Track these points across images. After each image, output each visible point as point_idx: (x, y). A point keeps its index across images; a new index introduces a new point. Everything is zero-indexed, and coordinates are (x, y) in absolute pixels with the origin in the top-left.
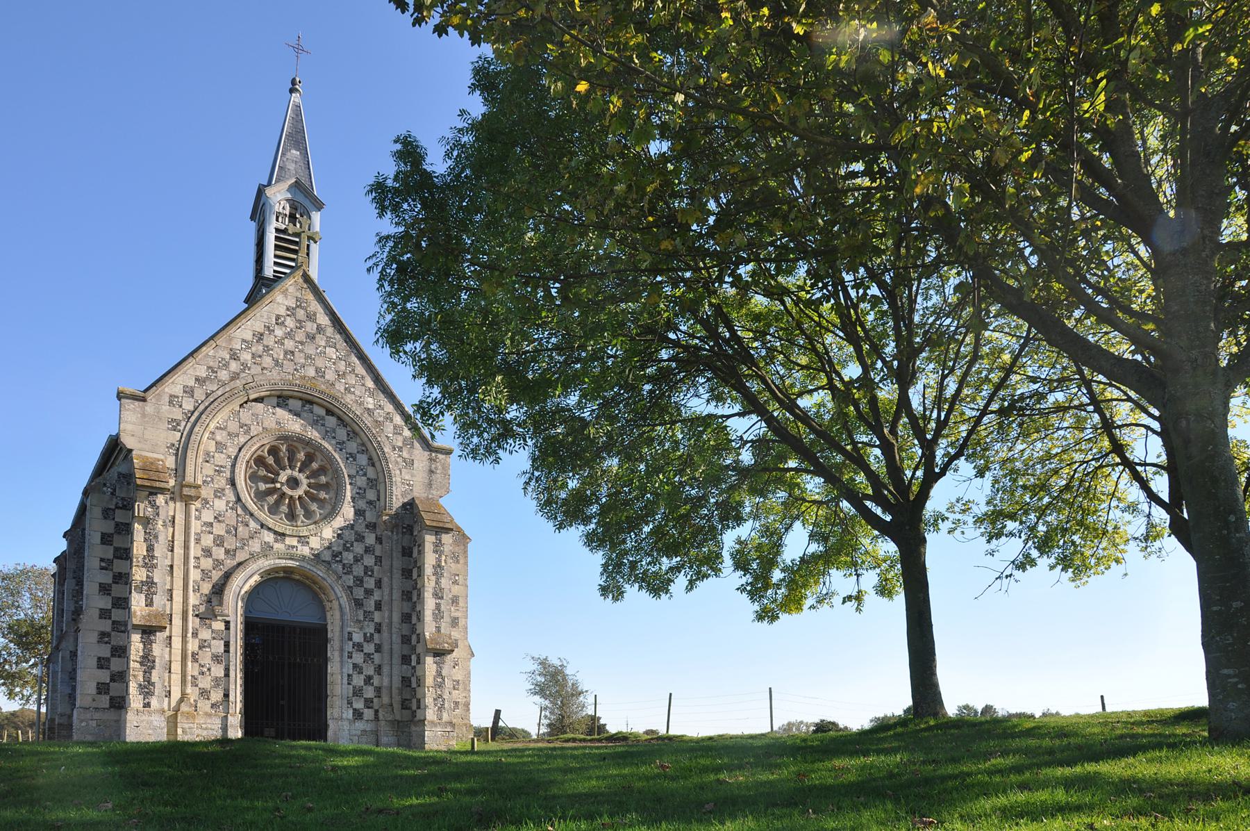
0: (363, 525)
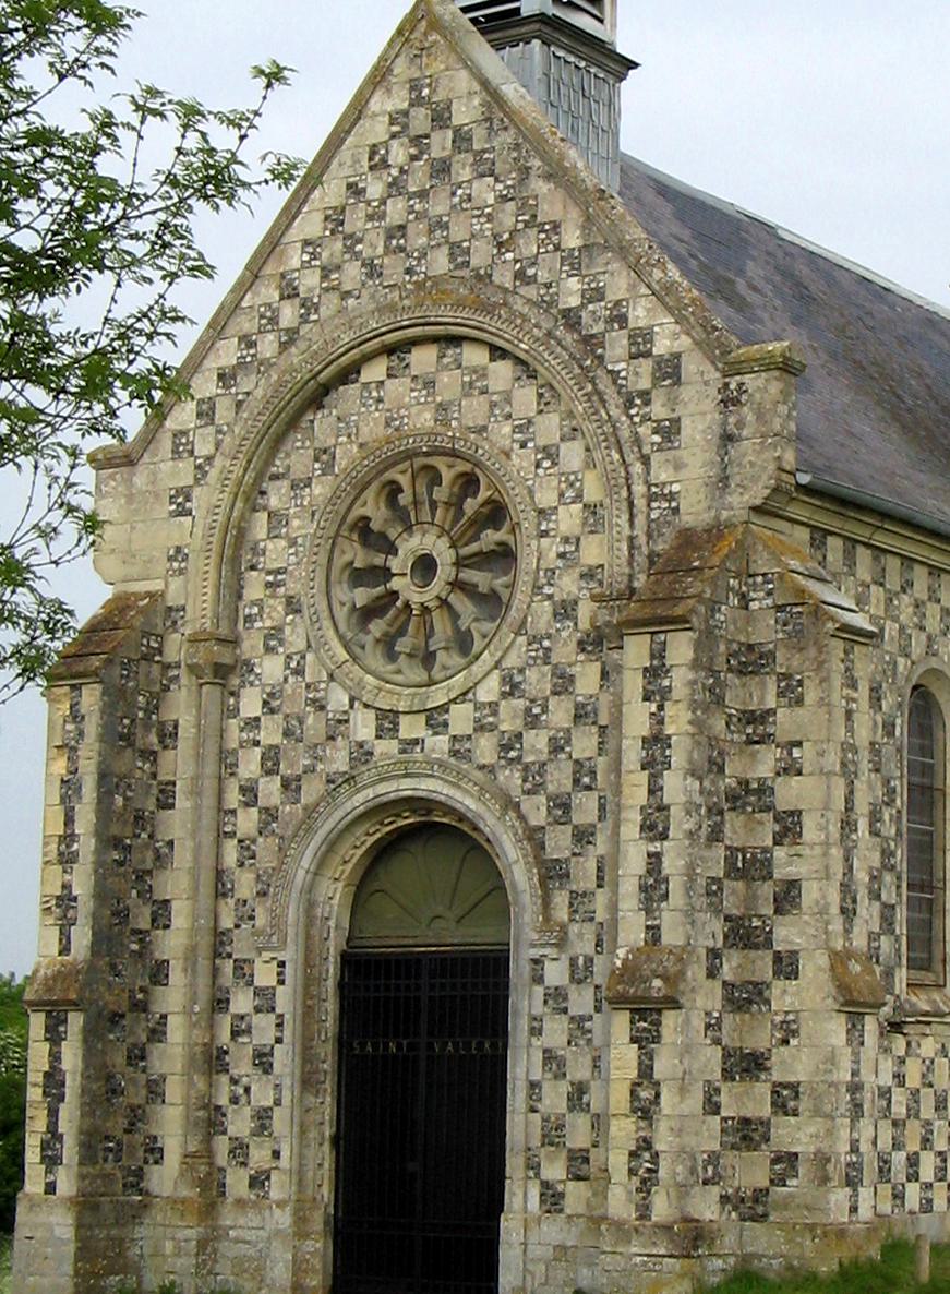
0: (573, 644)
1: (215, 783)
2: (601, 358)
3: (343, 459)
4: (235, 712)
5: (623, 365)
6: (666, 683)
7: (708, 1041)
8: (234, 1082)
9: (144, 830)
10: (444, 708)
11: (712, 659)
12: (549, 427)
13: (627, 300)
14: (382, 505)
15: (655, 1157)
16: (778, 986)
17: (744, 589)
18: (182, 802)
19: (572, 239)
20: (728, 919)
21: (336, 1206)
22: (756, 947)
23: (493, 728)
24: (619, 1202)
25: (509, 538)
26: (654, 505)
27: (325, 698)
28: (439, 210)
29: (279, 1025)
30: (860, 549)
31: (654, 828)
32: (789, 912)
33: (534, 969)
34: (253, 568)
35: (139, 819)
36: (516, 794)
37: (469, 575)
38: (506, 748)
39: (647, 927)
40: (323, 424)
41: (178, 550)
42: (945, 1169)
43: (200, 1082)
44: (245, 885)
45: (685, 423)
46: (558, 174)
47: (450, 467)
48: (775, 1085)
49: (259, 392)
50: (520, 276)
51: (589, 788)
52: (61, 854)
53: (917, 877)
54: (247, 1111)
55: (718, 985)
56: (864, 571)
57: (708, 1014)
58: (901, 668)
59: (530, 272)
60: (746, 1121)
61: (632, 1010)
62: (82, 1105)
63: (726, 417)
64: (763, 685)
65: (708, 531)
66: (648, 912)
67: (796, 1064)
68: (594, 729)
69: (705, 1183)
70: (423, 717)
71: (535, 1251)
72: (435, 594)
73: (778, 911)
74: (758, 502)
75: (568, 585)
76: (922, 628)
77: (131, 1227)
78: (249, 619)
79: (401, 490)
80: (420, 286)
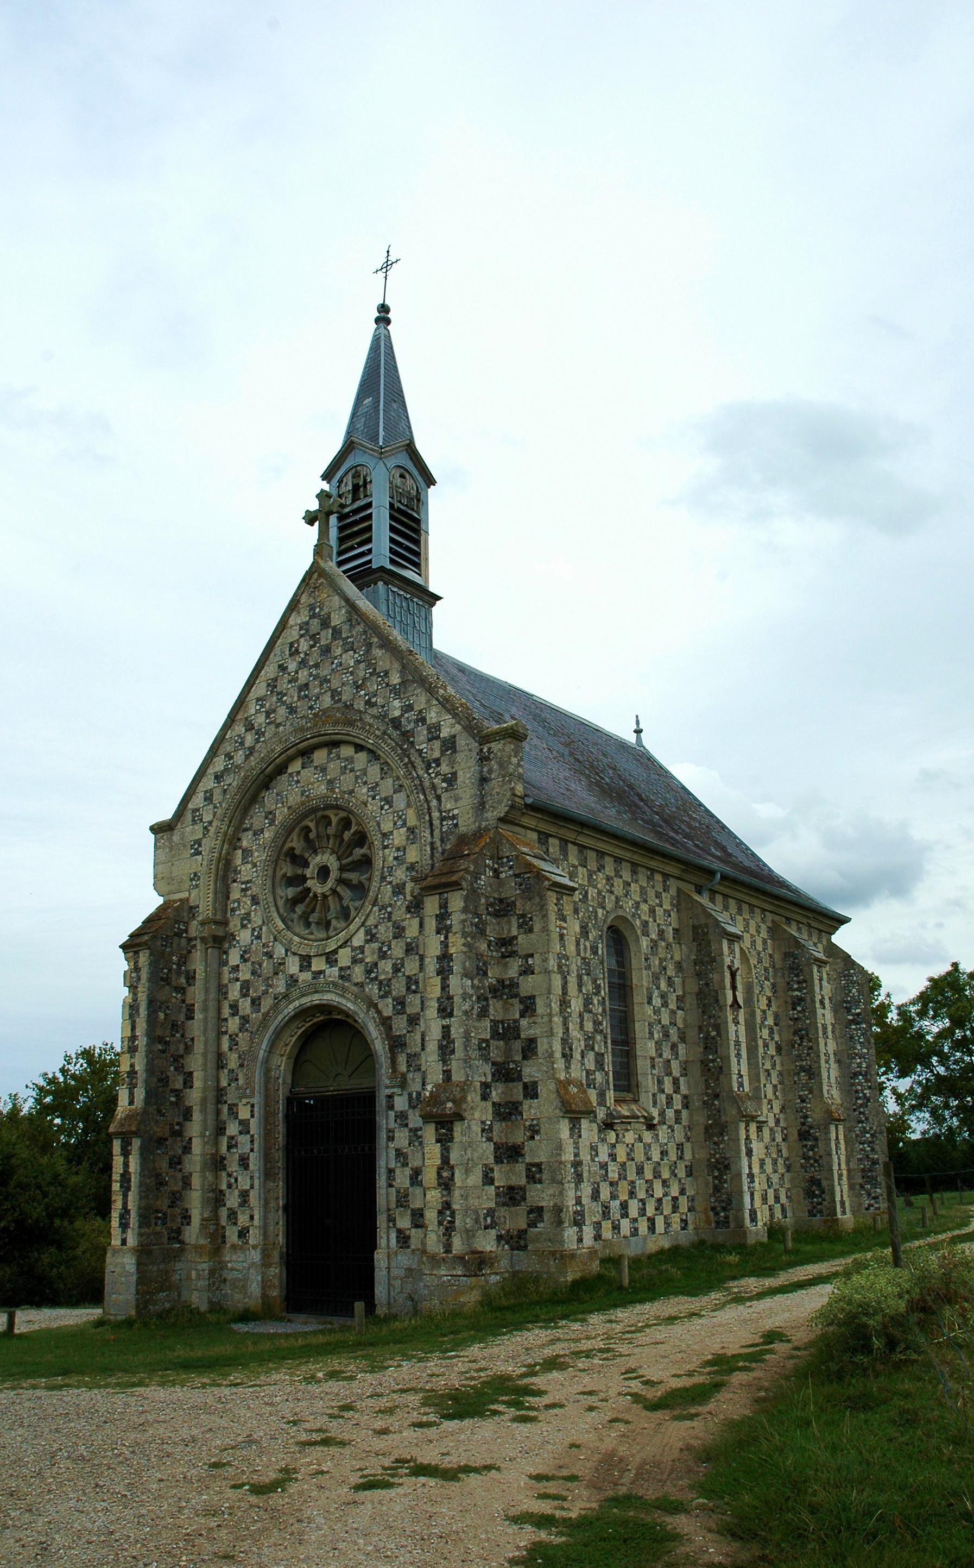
0: (404, 909)
1: (216, 1003)
2: (412, 743)
3: (279, 818)
4: (226, 963)
5: (425, 745)
6: (449, 922)
7: (484, 1139)
8: (229, 1175)
9: (177, 1032)
10: (335, 952)
11: (476, 907)
12: (387, 786)
13: (425, 709)
14: (302, 842)
15: (453, 1214)
16: (527, 1104)
17: (496, 866)
18: (198, 1016)
19: (395, 679)
20: (494, 1064)
21: (287, 1247)
22: (513, 1080)
23: (362, 961)
24: (433, 1242)
26: (445, 823)
27: (272, 951)
28: (325, 672)
29: (252, 1141)
30: (570, 845)
31: (445, 1011)
32: (531, 1058)
34: (235, 881)
35: (175, 1026)
36: (375, 999)
37: (346, 875)
38: (369, 972)
39: (444, 1071)
40: (269, 798)
41: (195, 874)
42: (645, 1209)
43: (210, 1176)
44: (233, 1061)
45: (460, 774)
46: (387, 644)
47: (336, 815)
48: (528, 1164)
49: (235, 783)
50: (368, 703)
51: (415, 992)
52: (129, 1047)
53: (619, 1037)
54: (236, 1192)
55: (489, 1104)
56: (573, 859)
57: (483, 1122)
58: (600, 915)
59: (374, 700)
60: (511, 1188)
61: (436, 1123)
62: (140, 1192)
63: (482, 768)
64: (509, 922)
65: (474, 835)
66: (444, 1062)
67: (538, 1152)
68: (417, 957)
69: (486, 1228)
70: (324, 958)
71: (395, 1272)
72: (329, 886)
73: (525, 1058)
74: (502, 815)
75: (400, 875)
76: (612, 892)
77: (172, 1263)
78: (233, 910)
79: (311, 831)
80: (316, 715)
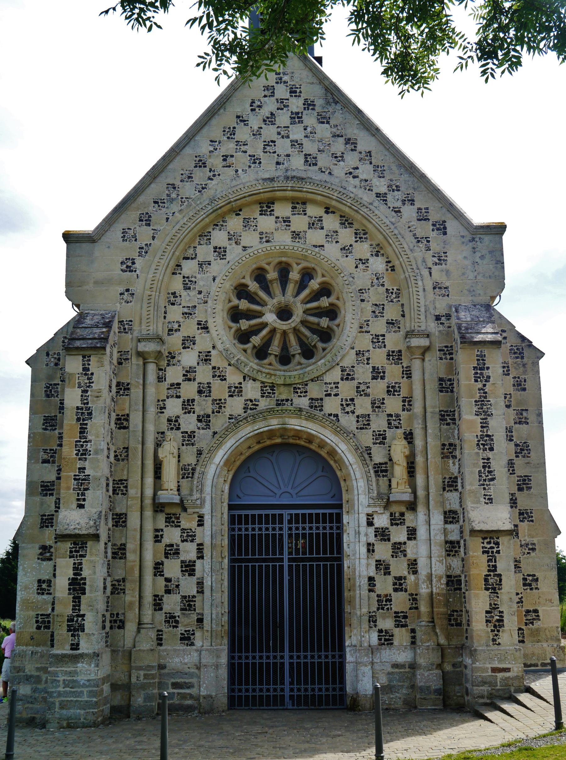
25: (336, 302)
33: (368, 519)
47: (298, 264)
